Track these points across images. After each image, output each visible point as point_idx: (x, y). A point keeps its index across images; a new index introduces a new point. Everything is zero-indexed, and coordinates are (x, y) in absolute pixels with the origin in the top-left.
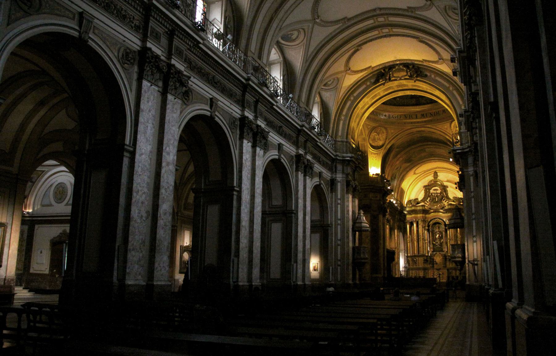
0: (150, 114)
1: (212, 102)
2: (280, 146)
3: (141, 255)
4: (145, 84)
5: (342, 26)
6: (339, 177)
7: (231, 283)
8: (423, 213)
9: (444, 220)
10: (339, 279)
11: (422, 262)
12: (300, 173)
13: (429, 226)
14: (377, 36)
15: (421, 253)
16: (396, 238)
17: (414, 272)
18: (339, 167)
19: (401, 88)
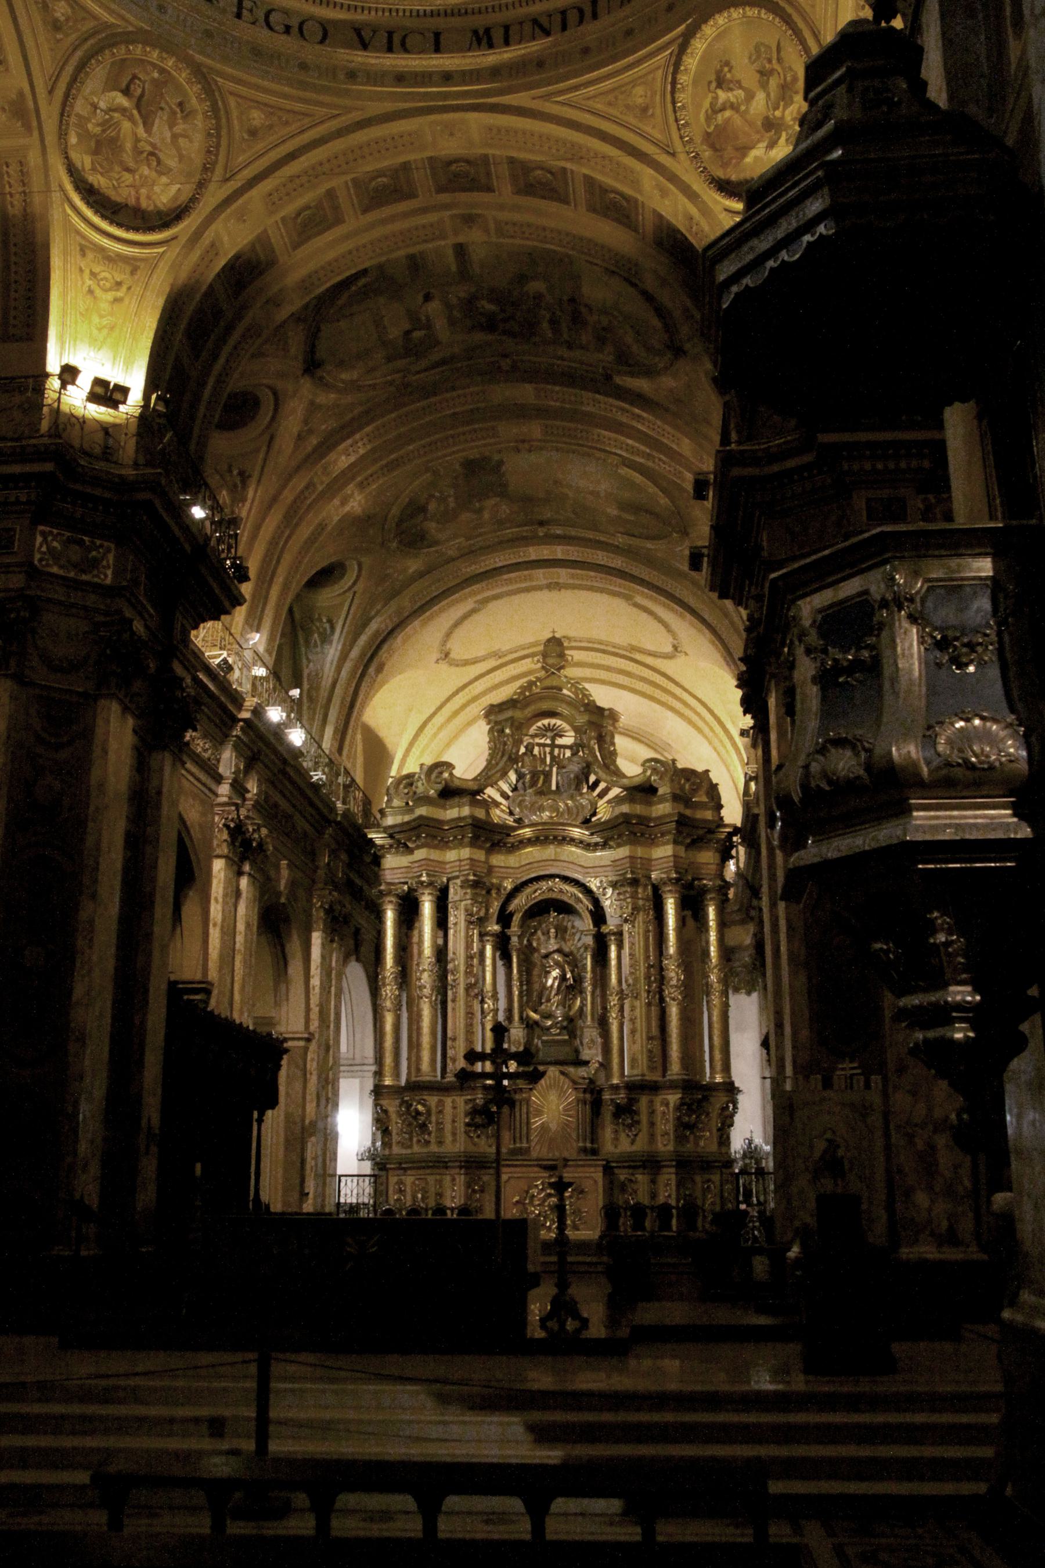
8: (474, 843)
9: (594, 884)
11: (463, 1119)
13: (505, 919)
16: (315, 981)
17: (409, 1180)
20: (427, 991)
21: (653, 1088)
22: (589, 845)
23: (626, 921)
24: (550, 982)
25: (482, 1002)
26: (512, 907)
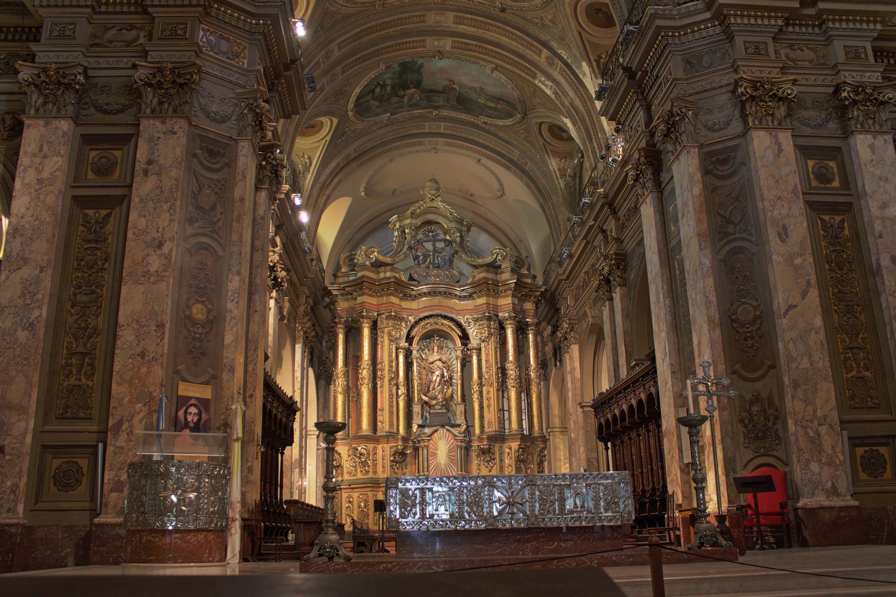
11: (389, 458)
13: (409, 339)
15: (384, 426)
17: (355, 495)
20: (366, 381)
22: (460, 297)
23: (484, 341)
24: (434, 378)
25: (398, 388)
26: (413, 333)
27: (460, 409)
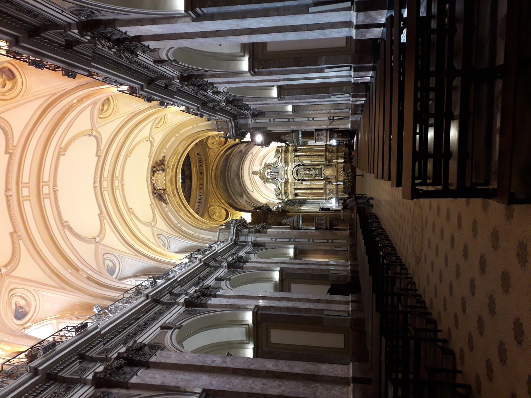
0: (168, 376)
1: (165, 327)
2: (218, 279)
3: (321, 387)
4: (134, 380)
5: (106, 220)
6: (251, 239)
7: (350, 317)
10: (346, 242)
11: (331, 186)
12: (245, 265)
13: (299, 180)
14: (121, 192)
15: (323, 187)
17: (339, 194)
18: (242, 239)
19: (174, 183)
21: (326, 157)
27: (317, 167)
